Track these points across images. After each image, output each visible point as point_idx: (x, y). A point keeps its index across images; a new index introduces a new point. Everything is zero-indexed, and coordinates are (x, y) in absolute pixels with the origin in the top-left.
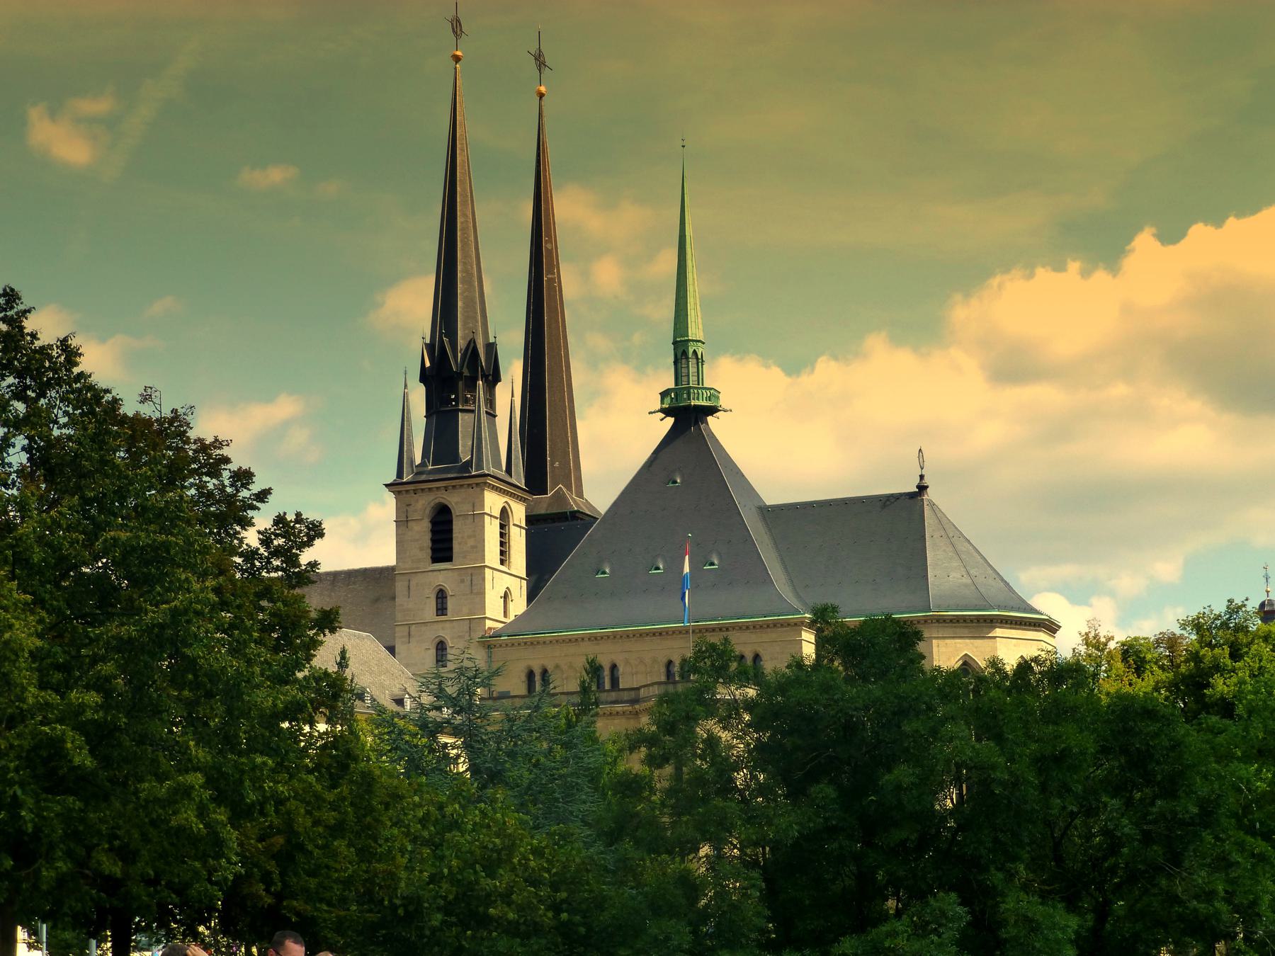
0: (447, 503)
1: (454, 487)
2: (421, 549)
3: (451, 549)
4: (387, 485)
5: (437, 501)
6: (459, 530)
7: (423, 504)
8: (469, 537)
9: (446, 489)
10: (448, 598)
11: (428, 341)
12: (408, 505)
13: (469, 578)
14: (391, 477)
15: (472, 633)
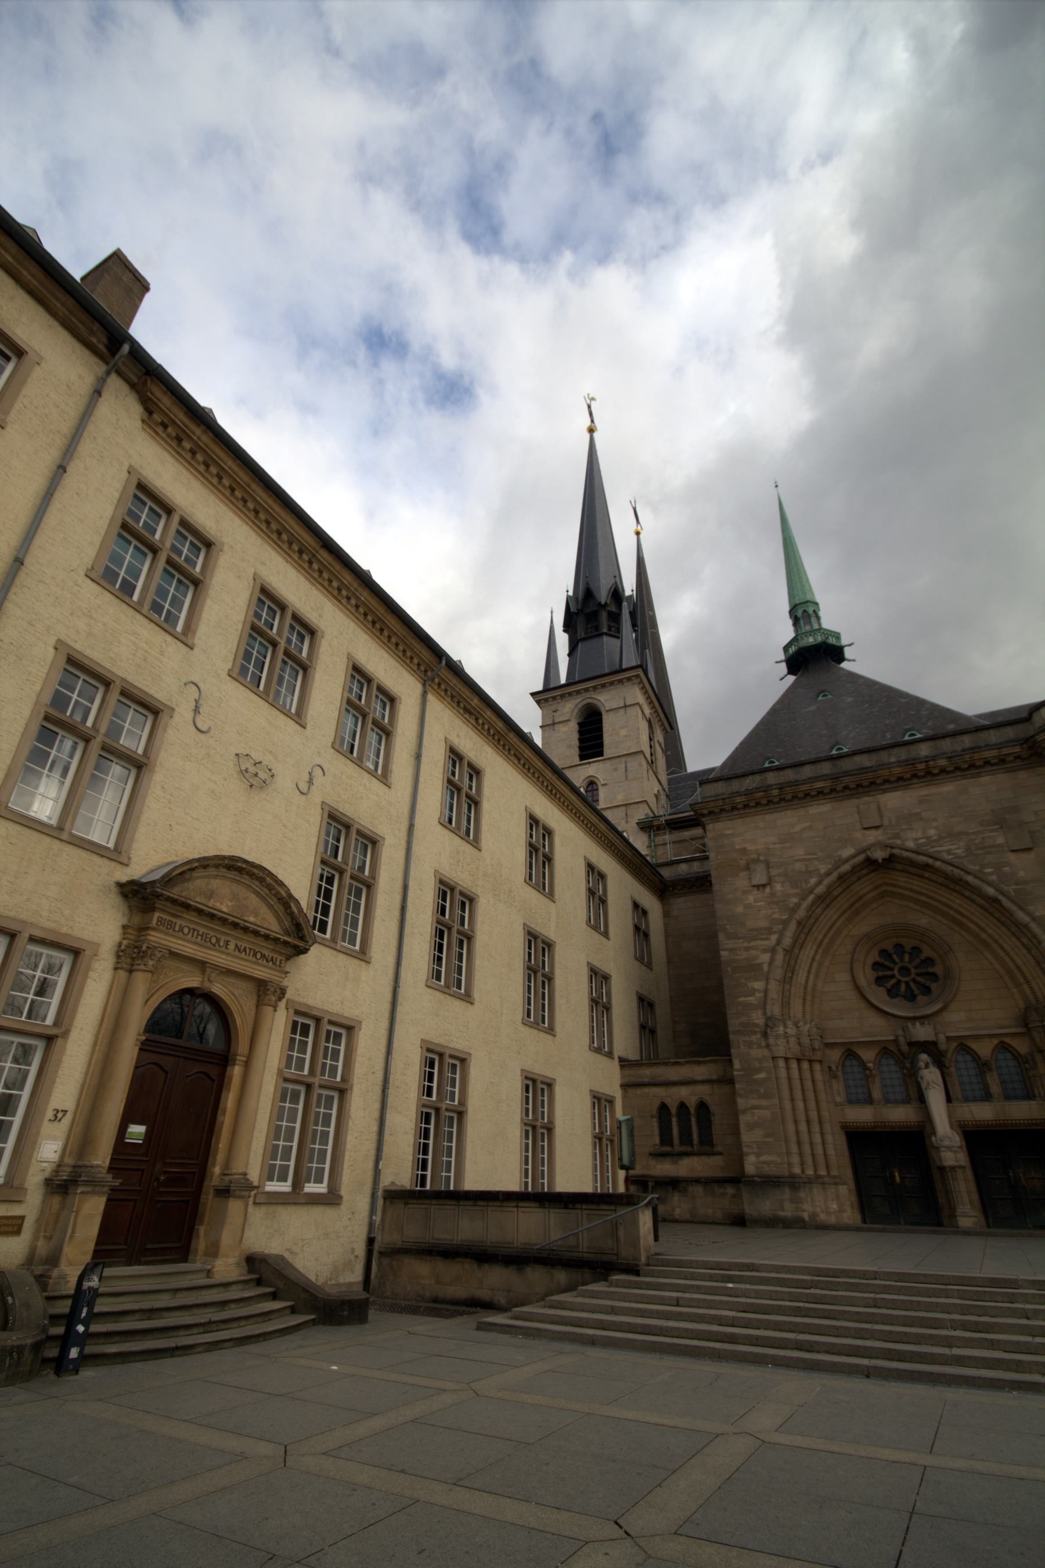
0: (595, 702)
1: (603, 686)
2: (569, 747)
3: (601, 745)
4: (533, 694)
5: (585, 702)
6: (609, 723)
7: (569, 709)
8: (623, 728)
9: (595, 688)
10: (600, 788)
11: (571, 593)
12: (555, 711)
13: (623, 766)
14: (540, 688)
15: (629, 819)
